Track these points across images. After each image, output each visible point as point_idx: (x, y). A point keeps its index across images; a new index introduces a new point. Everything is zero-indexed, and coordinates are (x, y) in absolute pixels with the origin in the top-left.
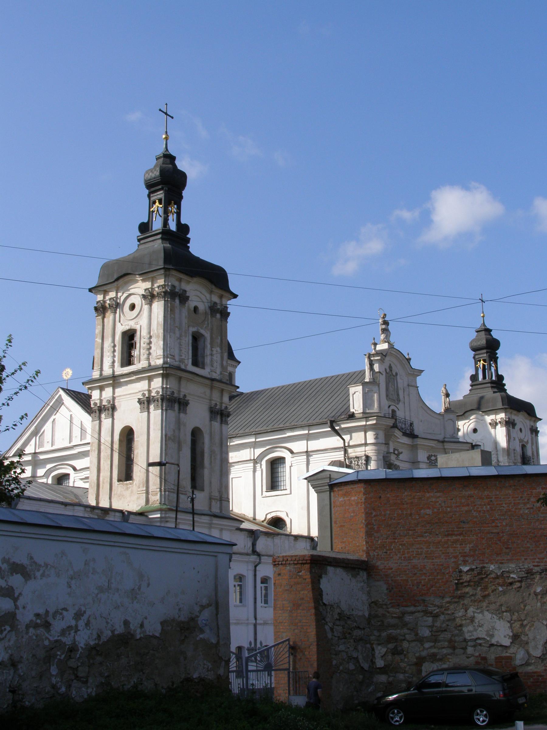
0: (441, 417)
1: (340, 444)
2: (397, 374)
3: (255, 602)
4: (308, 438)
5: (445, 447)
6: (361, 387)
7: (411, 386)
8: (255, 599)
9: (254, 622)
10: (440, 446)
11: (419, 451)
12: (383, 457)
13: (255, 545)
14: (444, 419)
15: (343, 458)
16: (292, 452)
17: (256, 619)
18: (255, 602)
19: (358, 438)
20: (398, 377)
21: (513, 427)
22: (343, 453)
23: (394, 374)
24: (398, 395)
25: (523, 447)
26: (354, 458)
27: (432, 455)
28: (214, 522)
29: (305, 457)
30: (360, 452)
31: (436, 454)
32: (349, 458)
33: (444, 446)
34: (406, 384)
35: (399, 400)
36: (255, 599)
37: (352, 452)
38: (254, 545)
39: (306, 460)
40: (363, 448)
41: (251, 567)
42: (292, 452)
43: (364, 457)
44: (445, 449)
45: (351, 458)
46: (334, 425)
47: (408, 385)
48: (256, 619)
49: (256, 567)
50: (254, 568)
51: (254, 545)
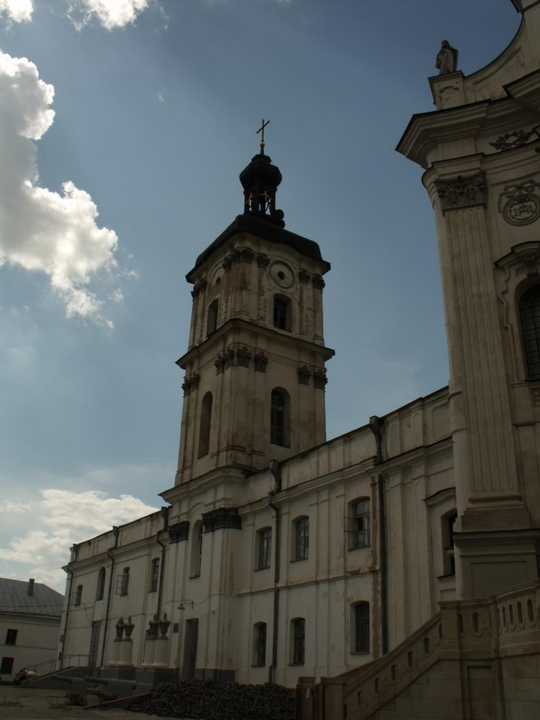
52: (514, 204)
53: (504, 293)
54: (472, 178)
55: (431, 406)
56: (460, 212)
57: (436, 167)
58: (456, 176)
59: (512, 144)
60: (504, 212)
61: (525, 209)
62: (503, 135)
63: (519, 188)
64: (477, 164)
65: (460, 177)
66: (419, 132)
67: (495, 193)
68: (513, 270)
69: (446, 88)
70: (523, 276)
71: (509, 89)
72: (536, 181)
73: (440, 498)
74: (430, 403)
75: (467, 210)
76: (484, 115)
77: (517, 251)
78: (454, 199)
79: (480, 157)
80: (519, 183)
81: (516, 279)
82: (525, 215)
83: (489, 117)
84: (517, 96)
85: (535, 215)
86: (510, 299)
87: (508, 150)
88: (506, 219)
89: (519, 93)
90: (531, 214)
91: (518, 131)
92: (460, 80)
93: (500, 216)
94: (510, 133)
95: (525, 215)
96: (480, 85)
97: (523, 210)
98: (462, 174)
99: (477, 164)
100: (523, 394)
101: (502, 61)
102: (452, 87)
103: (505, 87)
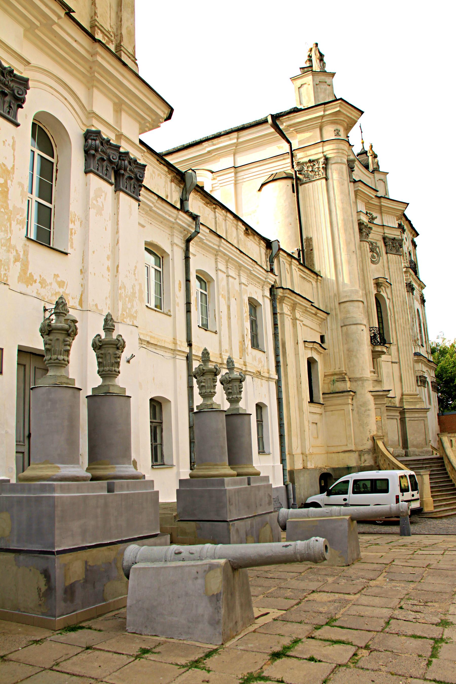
1: (285, 148)
3: (188, 311)
4: (236, 150)
5: (382, 204)
6: (311, 76)
8: (188, 304)
9: (187, 350)
10: (375, 201)
12: (347, 161)
13: (187, 200)
14: (374, 178)
15: (290, 168)
16: (212, 172)
17: (190, 345)
18: (188, 311)
19: (311, 136)
21: (403, 233)
22: (289, 160)
25: (410, 254)
26: (306, 163)
28: (99, 59)
29: (233, 174)
30: (315, 153)
31: (371, 212)
32: (298, 164)
33: (380, 202)
36: (188, 304)
37: (301, 156)
38: (183, 201)
39: (233, 178)
40: (320, 150)
41: (180, 242)
42: (212, 172)
43: (322, 160)
44: (381, 207)
45: (303, 163)
46: (278, 123)
48: (190, 345)
49: (188, 241)
50: (183, 246)
51: (183, 201)
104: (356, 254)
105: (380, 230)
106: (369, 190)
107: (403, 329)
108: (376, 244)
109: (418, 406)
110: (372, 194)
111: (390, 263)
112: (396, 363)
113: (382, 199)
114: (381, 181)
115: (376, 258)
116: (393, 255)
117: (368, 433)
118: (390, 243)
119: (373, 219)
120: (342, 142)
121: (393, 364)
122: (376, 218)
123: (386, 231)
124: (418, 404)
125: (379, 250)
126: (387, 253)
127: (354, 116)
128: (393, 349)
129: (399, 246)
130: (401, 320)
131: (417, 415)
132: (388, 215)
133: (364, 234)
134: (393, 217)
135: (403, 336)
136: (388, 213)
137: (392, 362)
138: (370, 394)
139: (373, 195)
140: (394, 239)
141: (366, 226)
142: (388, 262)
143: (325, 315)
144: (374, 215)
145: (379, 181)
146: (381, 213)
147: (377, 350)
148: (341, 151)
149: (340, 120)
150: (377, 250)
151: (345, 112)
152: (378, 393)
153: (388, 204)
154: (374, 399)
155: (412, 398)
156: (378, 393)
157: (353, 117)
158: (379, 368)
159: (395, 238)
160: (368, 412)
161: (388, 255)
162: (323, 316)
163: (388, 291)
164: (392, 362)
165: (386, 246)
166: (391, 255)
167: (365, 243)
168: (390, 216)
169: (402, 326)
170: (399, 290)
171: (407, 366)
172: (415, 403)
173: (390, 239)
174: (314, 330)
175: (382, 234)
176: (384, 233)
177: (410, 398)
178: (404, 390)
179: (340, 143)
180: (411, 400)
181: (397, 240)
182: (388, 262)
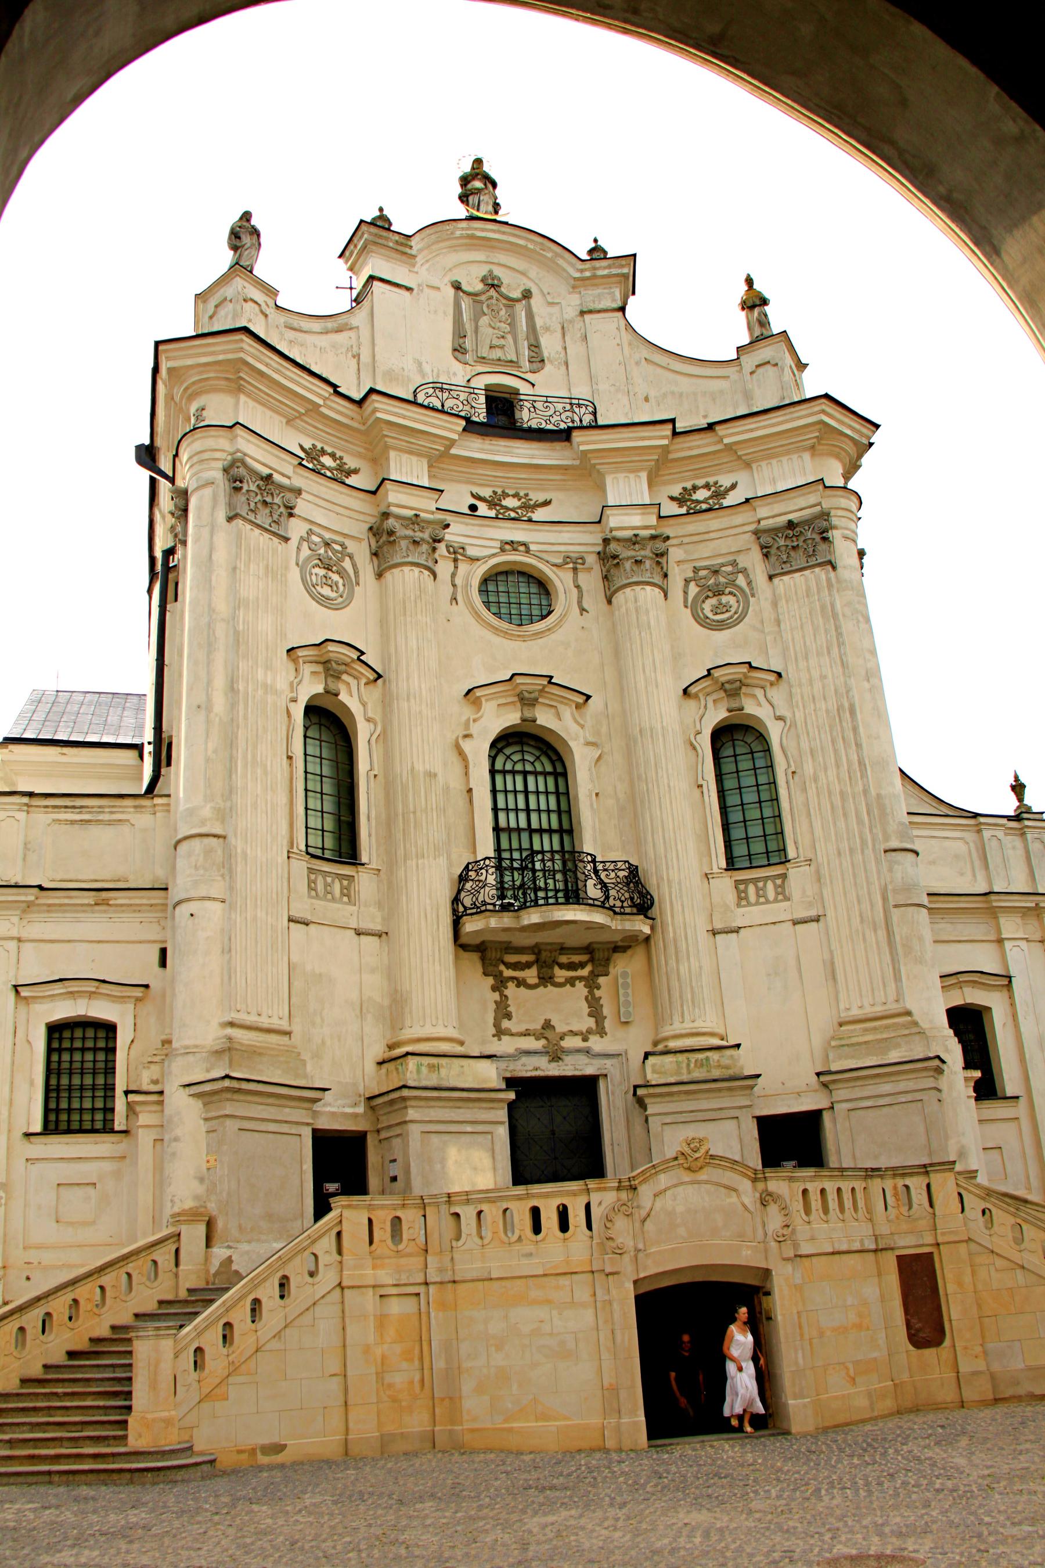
0: (730, 371)
2: (527, 295)
5: (726, 441)
7: (590, 312)
11: (609, 480)
12: (226, 470)
20: (536, 302)
23: (516, 294)
24: (535, 346)
27: (695, 488)
31: (711, 480)
34: (571, 312)
35: (538, 361)
47: (582, 313)
52: (317, 565)
53: (294, 700)
54: (281, 487)
55: (47, 813)
56: (257, 531)
57: (238, 430)
58: (266, 472)
59: (328, 469)
60: (302, 567)
61: (330, 582)
62: (319, 446)
63: (327, 545)
64: (289, 470)
65: (269, 477)
66: (230, 356)
67: (296, 529)
68: (307, 669)
69: (252, 300)
70: (320, 689)
71: (374, 397)
72: (349, 550)
73: (58, 989)
74: (46, 807)
75: (267, 536)
76: (321, 402)
77: (332, 647)
78: (252, 505)
79: (296, 461)
80: (328, 536)
81: (312, 687)
82: (326, 591)
83: (323, 410)
84: (379, 415)
85: (340, 600)
86: (298, 712)
87: (319, 473)
88: (304, 580)
89: (383, 410)
90: (333, 595)
91: (338, 454)
92: (271, 303)
93: (297, 570)
94: (329, 450)
95: (326, 591)
96: (291, 335)
97: (326, 581)
98: (277, 477)
99: (289, 470)
100: (301, 866)
101: (330, 324)
102: (259, 305)
103: (372, 391)
104: (209, 709)
105: (743, 517)
106: (631, 435)
107: (837, 800)
108: (734, 563)
109: (894, 1056)
110: (661, 437)
111: (782, 603)
112: (817, 919)
113: (717, 428)
114: (768, 367)
115: (733, 610)
116: (797, 575)
117: (169, 1204)
118: (782, 542)
119: (720, 494)
120: (196, 436)
121: (798, 927)
122: (733, 486)
123: (763, 511)
124: (898, 1046)
125: (747, 576)
126: (771, 578)
127: (224, 352)
128: (797, 877)
129: (817, 538)
130: (832, 773)
131: (887, 1088)
132: (774, 462)
133: (628, 565)
134: (795, 457)
135: (841, 824)
136: (770, 455)
137: (795, 923)
138: (184, 1093)
139: (663, 437)
140: (791, 525)
141: (634, 541)
142: (775, 604)
143: (162, 893)
144: (725, 481)
145: (761, 370)
146: (748, 465)
147: (526, 922)
148: (195, 459)
149: (194, 383)
150: (741, 580)
151: (189, 362)
152: (207, 1087)
153: (751, 430)
154: (205, 1105)
155: (866, 1030)
156: (207, 1087)
157: (221, 357)
158: (672, 963)
159: (790, 522)
160: (174, 1144)
161: (776, 581)
162: (159, 898)
163: (777, 694)
164: (795, 923)
165: (766, 556)
166: (786, 578)
167: (628, 590)
168: (784, 459)
169: (836, 788)
170: (823, 677)
171: (856, 921)
172: (885, 1045)
173: (774, 531)
174: (107, 942)
175: (753, 527)
176: (759, 522)
177: (866, 1030)
178: (842, 1007)
179: (193, 442)
180: (869, 1037)
181: (808, 522)
182: (775, 604)
